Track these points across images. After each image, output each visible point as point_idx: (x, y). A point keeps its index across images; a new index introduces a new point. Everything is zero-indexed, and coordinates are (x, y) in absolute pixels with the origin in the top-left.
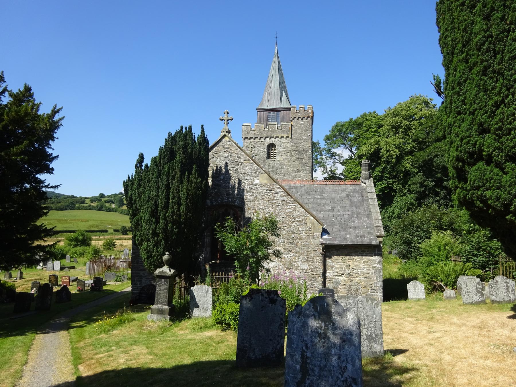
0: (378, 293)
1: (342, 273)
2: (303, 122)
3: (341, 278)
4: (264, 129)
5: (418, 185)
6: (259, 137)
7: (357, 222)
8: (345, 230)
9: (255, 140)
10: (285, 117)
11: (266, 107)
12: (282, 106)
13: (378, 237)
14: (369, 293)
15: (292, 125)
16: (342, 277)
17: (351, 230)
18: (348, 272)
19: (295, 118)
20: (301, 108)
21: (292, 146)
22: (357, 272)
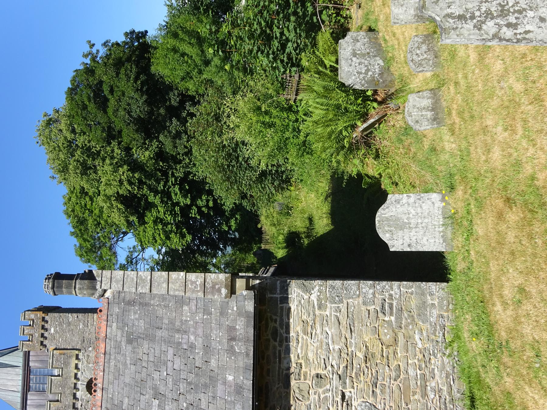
0: (391, 295)
1: (339, 399)
2: (52, 330)
3: (354, 403)
5: (178, 141)
7: (192, 338)
8: (213, 380)
10: (41, 358)
11: (19, 395)
12: (21, 364)
13: (232, 291)
14: (393, 318)
15: (56, 349)
16: (351, 398)
17: (213, 363)
18: (335, 381)
19: (42, 342)
20: (26, 332)
22: (336, 355)
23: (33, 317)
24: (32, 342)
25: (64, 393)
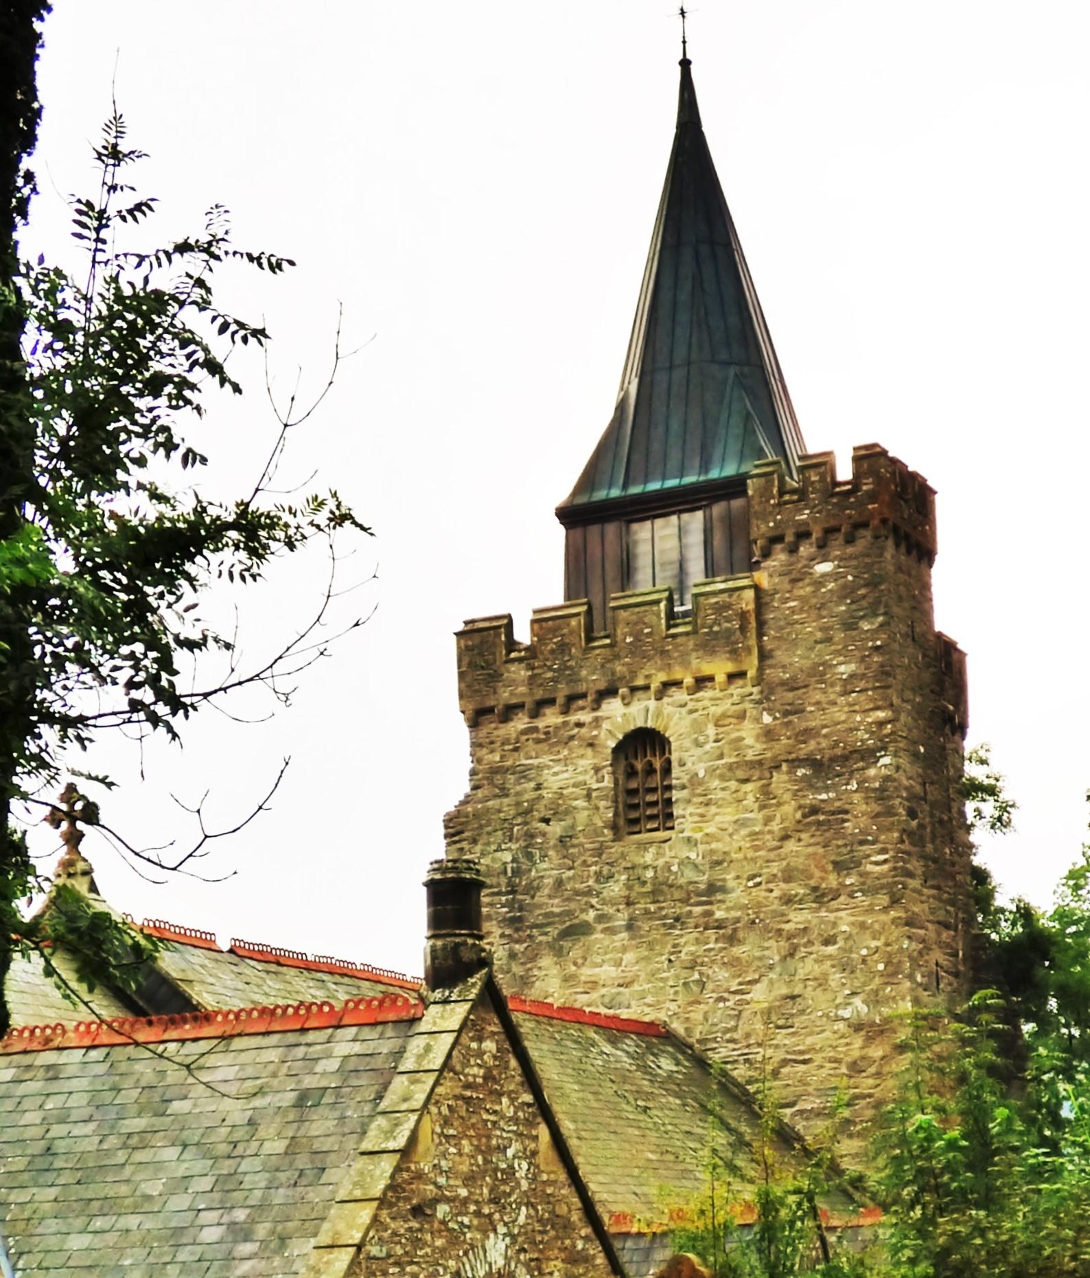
4: (590, 639)
6: (560, 700)
9: (541, 723)
21: (769, 734)
23: (865, 488)
24: (779, 505)
25: (617, 657)
